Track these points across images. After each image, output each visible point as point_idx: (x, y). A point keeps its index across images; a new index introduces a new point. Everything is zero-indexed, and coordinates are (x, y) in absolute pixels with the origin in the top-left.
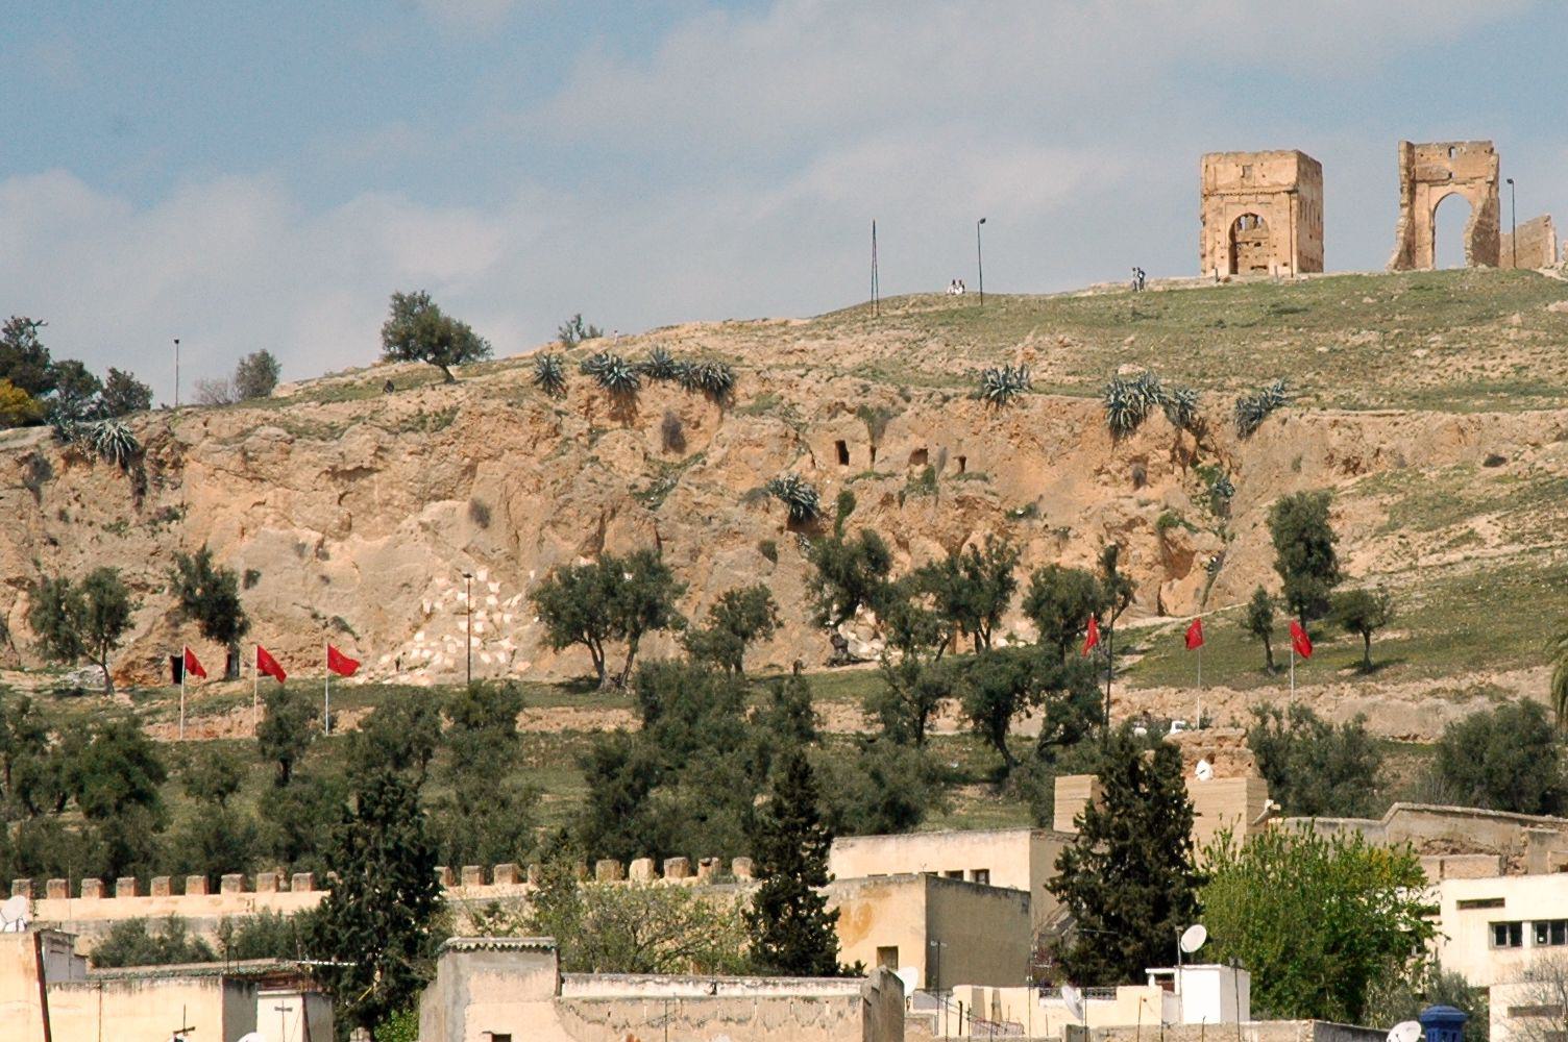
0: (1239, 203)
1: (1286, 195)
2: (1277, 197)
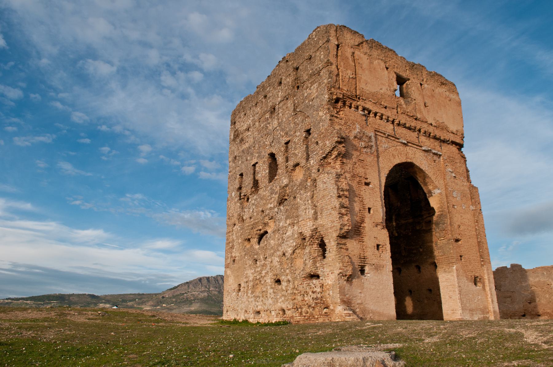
1: (454, 149)
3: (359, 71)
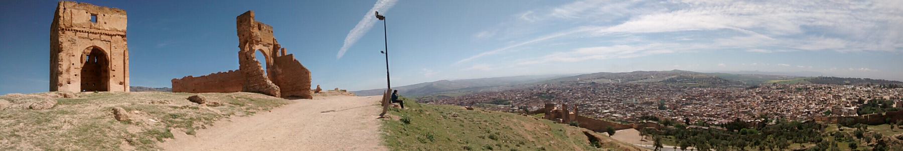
0: (88, 38)
1: (120, 37)
2: (113, 37)
3: (73, 16)
